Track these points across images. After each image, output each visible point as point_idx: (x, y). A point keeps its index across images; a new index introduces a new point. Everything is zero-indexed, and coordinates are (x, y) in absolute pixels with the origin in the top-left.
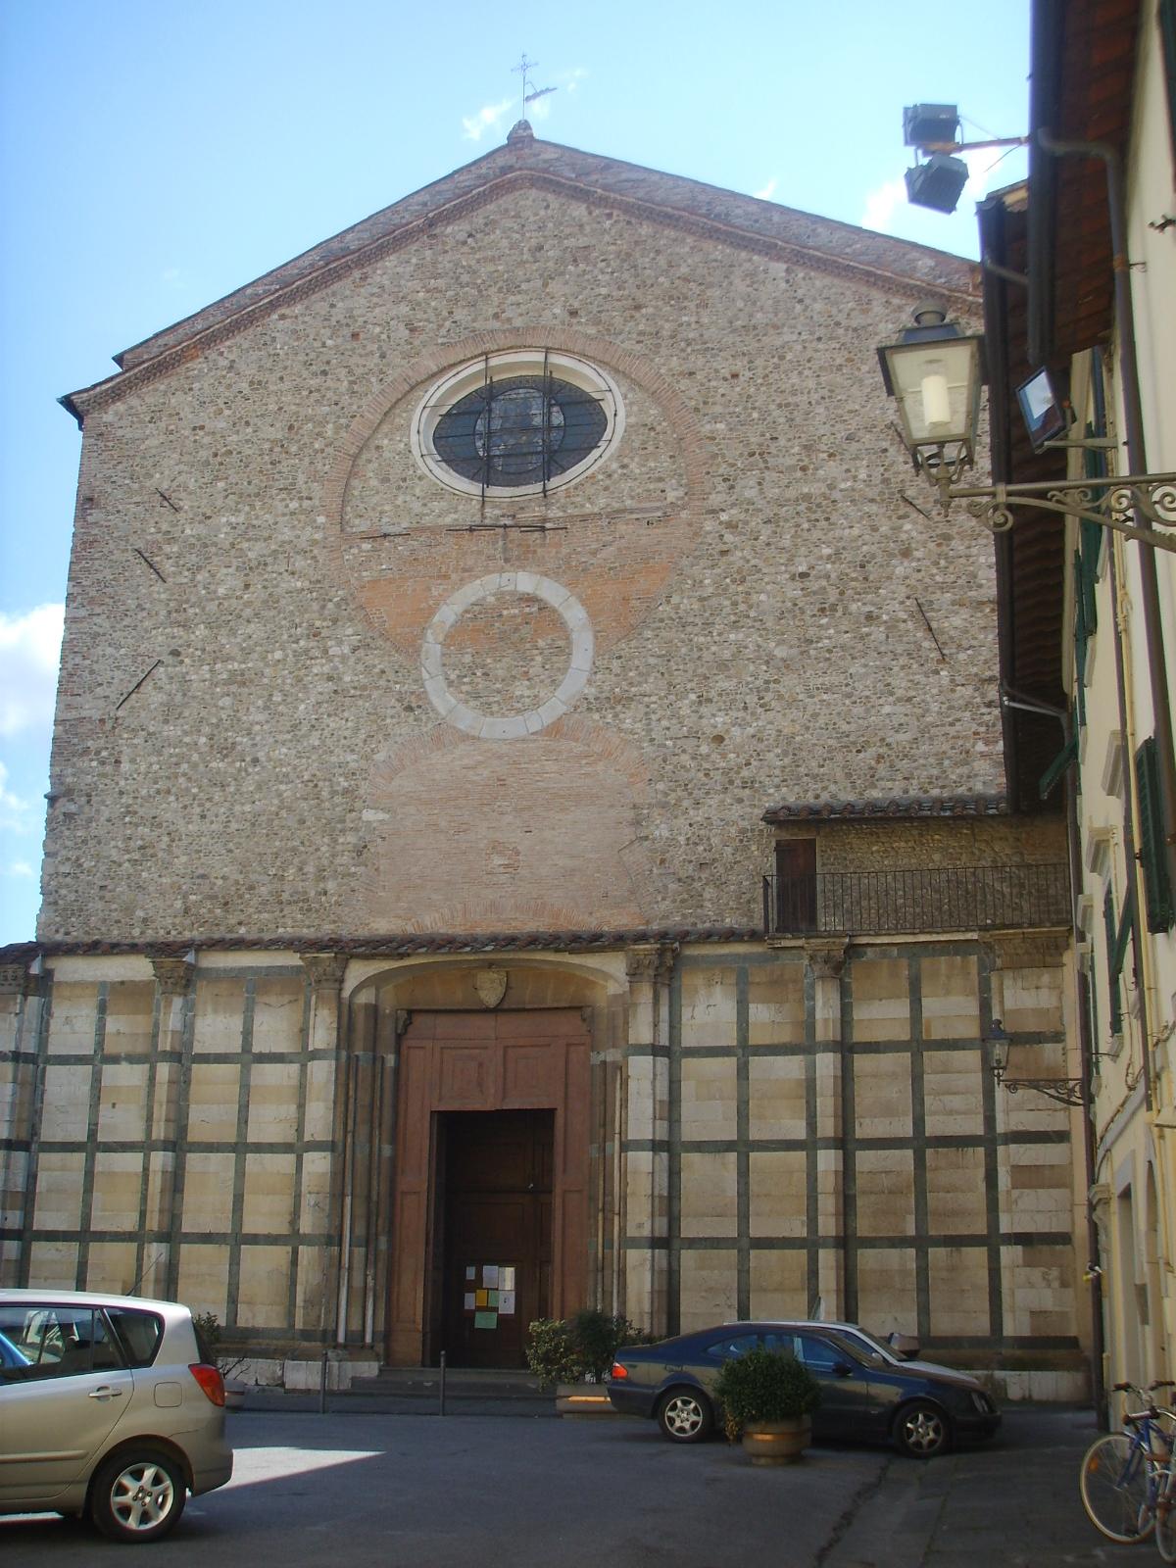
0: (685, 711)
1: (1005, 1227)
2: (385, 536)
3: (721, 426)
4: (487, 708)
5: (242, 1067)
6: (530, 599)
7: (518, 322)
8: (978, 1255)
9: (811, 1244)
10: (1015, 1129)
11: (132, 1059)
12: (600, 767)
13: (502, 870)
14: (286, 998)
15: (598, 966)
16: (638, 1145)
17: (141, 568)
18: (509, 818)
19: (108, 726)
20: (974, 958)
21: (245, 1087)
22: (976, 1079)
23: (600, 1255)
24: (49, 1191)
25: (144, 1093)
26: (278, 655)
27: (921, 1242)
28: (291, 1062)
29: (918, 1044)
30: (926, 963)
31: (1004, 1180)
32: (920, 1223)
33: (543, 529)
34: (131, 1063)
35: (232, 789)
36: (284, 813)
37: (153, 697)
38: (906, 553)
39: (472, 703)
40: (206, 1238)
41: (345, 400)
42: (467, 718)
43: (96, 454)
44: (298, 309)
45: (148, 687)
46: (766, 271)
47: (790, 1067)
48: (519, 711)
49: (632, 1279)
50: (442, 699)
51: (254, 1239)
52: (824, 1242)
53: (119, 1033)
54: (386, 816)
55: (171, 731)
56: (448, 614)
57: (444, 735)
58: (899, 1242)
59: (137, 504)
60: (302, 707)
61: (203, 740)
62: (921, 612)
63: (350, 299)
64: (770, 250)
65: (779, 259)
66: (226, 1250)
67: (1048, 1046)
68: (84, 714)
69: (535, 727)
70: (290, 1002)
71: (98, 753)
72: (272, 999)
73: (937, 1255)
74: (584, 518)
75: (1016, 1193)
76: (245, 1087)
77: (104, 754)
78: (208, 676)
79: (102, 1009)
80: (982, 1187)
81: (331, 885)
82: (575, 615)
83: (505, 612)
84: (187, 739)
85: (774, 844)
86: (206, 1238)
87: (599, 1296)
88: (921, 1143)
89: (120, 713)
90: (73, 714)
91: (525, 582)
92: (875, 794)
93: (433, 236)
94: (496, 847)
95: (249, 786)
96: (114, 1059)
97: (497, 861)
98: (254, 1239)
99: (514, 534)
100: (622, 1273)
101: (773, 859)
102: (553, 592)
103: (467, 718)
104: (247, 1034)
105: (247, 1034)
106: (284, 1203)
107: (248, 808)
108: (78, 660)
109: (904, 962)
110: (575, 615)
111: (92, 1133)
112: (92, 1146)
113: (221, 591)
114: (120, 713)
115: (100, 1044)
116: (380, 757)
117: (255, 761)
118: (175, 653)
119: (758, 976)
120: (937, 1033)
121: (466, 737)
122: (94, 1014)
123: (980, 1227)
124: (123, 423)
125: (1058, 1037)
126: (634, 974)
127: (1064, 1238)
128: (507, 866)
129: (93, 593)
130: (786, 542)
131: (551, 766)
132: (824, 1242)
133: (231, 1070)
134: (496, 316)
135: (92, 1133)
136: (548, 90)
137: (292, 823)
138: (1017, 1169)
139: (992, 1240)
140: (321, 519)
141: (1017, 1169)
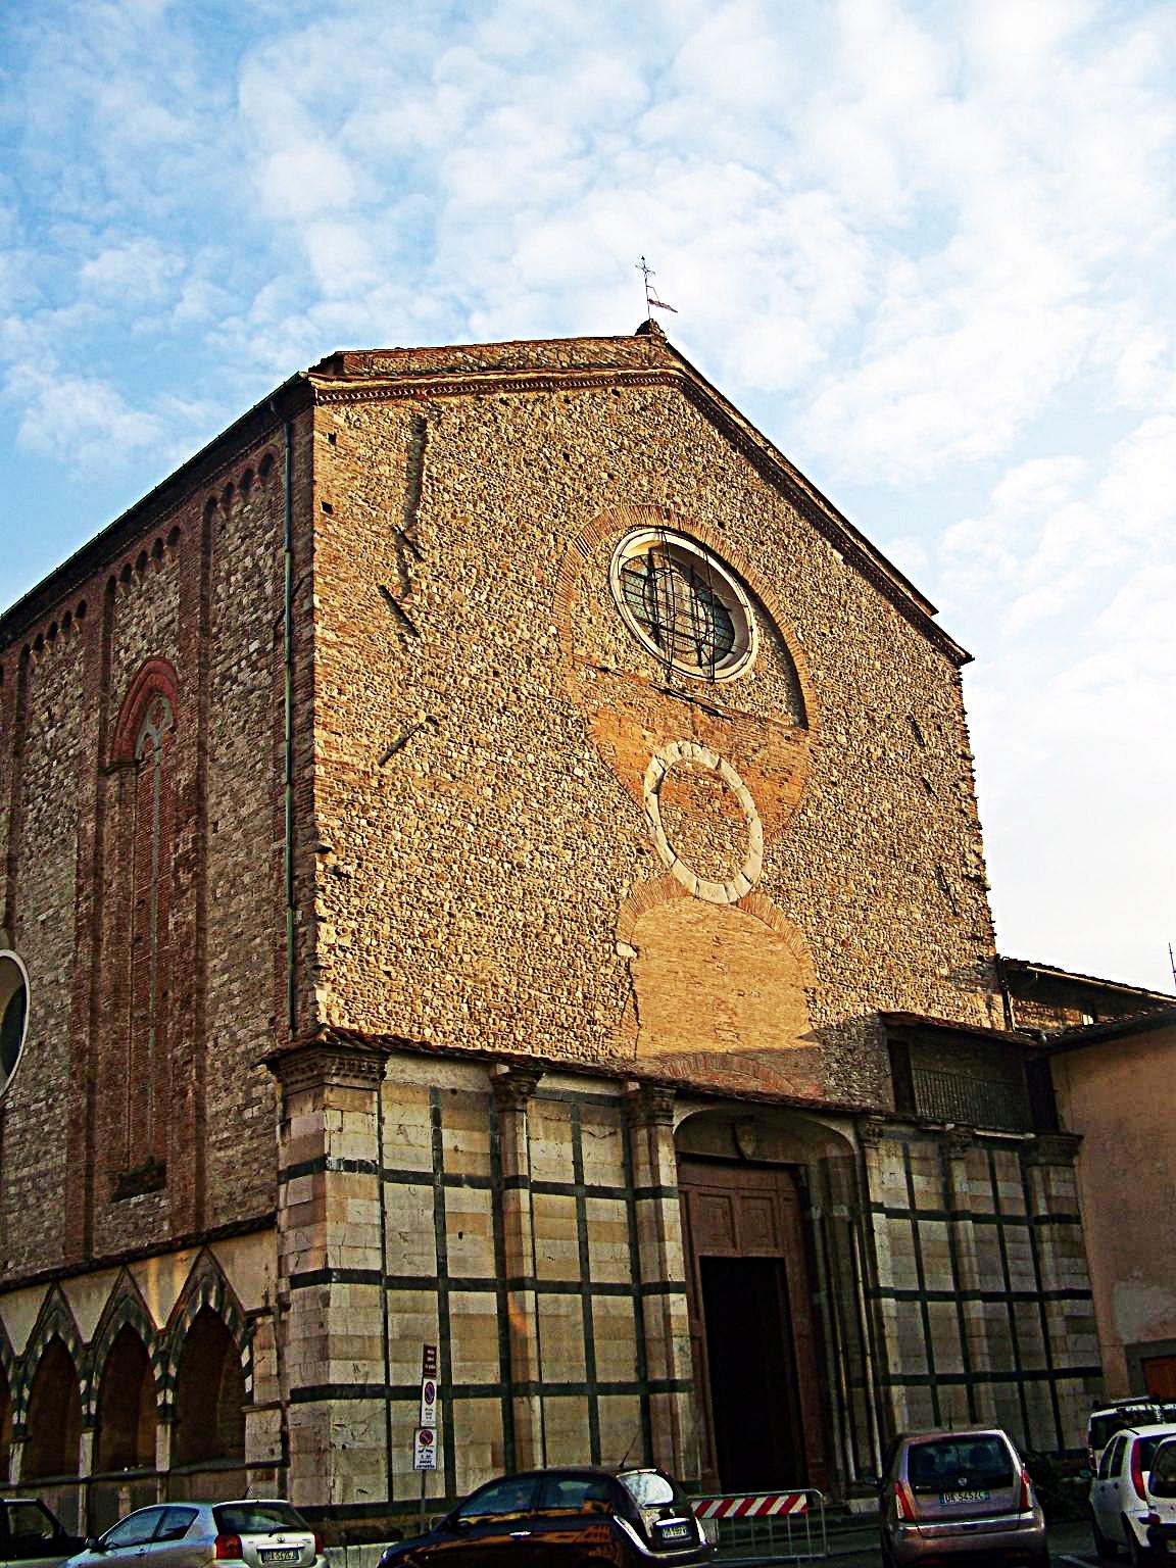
0: (825, 913)
1: (1062, 1363)
2: (606, 670)
3: (820, 673)
4: (696, 869)
5: (577, 1200)
6: (717, 778)
7: (683, 511)
8: (1045, 1384)
9: (971, 1378)
10: (1069, 1287)
11: (475, 1182)
12: (780, 946)
13: (725, 1027)
14: (607, 1130)
15: (837, 1129)
16: (889, 1293)
17: (387, 611)
18: (726, 979)
19: (374, 783)
20: (1017, 1154)
21: (582, 1221)
22: (1027, 1249)
23: (845, 1394)
24: (403, 1337)
25: (489, 1222)
26: (531, 758)
27: (1019, 1377)
28: (618, 1198)
29: (1000, 1219)
30: (996, 1154)
31: (1057, 1326)
32: (1018, 1365)
33: (717, 714)
34: (473, 1187)
35: (503, 890)
36: (552, 931)
37: (415, 764)
38: (930, 825)
39: (689, 862)
40: (565, 1389)
41: (563, 518)
42: (682, 872)
43: (328, 455)
44: (515, 399)
45: (409, 749)
46: (832, 554)
47: (939, 1228)
48: (720, 879)
49: (897, 1412)
50: (663, 848)
51: (608, 1389)
52: (982, 1377)
53: (456, 1149)
54: (630, 953)
55: (440, 810)
56: (655, 768)
57: (670, 887)
58: (1009, 1377)
59: (378, 534)
60: (557, 821)
61: (470, 828)
62: (940, 872)
63: (557, 412)
64: (838, 540)
65: (840, 551)
66: (584, 1401)
67: (1075, 1226)
68: (346, 759)
69: (734, 898)
70: (610, 1134)
71: (365, 809)
72: (595, 1130)
73: (1027, 1384)
74: (744, 716)
75: (1073, 1337)
76: (582, 1221)
77: (374, 814)
78: (466, 759)
79: (436, 1119)
80: (1041, 1335)
81: (598, 1015)
82: (748, 802)
83: (701, 782)
84: (458, 824)
85: (886, 1043)
86: (565, 1389)
87: (848, 1432)
88: (1009, 1297)
89: (387, 771)
90: (335, 756)
91: (706, 758)
92: (934, 1013)
93: (615, 392)
94: (720, 1004)
95: (517, 893)
96: (456, 1181)
97: (724, 1018)
98: (608, 1389)
99: (699, 711)
100: (885, 1406)
101: (885, 1056)
102: (728, 770)
103: (682, 872)
104: (578, 1163)
105: (578, 1163)
106: (629, 1349)
107: (519, 915)
108: (335, 693)
109: (985, 1152)
110: (748, 802)
111: (442, 1268)
112: (442, 1283)
113: (474, 670)
114: (387, 771)
115: (438, 1161)
116: (624, 892)
117: (520, 866)
118: (429, 719)
119: (915, 1150)
120: (1007, 1211)
121: (686, 893)
122: (429, 1124)
123: (1044, 1366)
124: (354, 433)
125: (1078, 1220)
126: (860, 1141)
127: (1097, 1372)
128: (730, 1024)
129: (341, 618)
130: (866, 790)
131: (748, 938)
132: (982, 1377)
133: (569, 1201)
134: (667, 496)
135: (442, 1268)
136: (668, 307)
137: (558, 940)
138: (1068, 1319)
139: (1053, 1375)
140: (553, 630)
141: (1068, 1319)
